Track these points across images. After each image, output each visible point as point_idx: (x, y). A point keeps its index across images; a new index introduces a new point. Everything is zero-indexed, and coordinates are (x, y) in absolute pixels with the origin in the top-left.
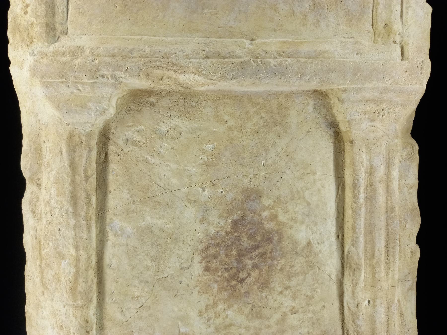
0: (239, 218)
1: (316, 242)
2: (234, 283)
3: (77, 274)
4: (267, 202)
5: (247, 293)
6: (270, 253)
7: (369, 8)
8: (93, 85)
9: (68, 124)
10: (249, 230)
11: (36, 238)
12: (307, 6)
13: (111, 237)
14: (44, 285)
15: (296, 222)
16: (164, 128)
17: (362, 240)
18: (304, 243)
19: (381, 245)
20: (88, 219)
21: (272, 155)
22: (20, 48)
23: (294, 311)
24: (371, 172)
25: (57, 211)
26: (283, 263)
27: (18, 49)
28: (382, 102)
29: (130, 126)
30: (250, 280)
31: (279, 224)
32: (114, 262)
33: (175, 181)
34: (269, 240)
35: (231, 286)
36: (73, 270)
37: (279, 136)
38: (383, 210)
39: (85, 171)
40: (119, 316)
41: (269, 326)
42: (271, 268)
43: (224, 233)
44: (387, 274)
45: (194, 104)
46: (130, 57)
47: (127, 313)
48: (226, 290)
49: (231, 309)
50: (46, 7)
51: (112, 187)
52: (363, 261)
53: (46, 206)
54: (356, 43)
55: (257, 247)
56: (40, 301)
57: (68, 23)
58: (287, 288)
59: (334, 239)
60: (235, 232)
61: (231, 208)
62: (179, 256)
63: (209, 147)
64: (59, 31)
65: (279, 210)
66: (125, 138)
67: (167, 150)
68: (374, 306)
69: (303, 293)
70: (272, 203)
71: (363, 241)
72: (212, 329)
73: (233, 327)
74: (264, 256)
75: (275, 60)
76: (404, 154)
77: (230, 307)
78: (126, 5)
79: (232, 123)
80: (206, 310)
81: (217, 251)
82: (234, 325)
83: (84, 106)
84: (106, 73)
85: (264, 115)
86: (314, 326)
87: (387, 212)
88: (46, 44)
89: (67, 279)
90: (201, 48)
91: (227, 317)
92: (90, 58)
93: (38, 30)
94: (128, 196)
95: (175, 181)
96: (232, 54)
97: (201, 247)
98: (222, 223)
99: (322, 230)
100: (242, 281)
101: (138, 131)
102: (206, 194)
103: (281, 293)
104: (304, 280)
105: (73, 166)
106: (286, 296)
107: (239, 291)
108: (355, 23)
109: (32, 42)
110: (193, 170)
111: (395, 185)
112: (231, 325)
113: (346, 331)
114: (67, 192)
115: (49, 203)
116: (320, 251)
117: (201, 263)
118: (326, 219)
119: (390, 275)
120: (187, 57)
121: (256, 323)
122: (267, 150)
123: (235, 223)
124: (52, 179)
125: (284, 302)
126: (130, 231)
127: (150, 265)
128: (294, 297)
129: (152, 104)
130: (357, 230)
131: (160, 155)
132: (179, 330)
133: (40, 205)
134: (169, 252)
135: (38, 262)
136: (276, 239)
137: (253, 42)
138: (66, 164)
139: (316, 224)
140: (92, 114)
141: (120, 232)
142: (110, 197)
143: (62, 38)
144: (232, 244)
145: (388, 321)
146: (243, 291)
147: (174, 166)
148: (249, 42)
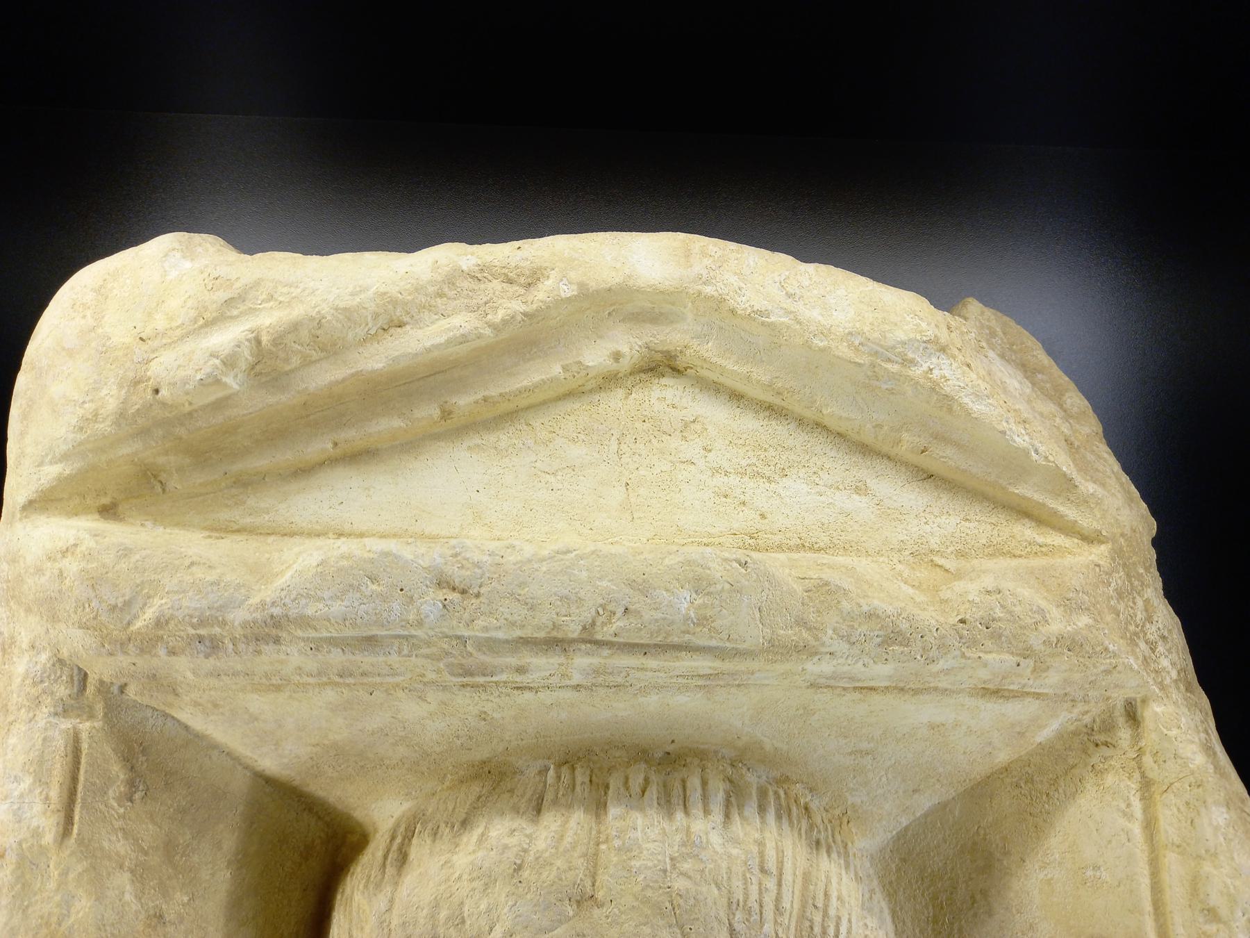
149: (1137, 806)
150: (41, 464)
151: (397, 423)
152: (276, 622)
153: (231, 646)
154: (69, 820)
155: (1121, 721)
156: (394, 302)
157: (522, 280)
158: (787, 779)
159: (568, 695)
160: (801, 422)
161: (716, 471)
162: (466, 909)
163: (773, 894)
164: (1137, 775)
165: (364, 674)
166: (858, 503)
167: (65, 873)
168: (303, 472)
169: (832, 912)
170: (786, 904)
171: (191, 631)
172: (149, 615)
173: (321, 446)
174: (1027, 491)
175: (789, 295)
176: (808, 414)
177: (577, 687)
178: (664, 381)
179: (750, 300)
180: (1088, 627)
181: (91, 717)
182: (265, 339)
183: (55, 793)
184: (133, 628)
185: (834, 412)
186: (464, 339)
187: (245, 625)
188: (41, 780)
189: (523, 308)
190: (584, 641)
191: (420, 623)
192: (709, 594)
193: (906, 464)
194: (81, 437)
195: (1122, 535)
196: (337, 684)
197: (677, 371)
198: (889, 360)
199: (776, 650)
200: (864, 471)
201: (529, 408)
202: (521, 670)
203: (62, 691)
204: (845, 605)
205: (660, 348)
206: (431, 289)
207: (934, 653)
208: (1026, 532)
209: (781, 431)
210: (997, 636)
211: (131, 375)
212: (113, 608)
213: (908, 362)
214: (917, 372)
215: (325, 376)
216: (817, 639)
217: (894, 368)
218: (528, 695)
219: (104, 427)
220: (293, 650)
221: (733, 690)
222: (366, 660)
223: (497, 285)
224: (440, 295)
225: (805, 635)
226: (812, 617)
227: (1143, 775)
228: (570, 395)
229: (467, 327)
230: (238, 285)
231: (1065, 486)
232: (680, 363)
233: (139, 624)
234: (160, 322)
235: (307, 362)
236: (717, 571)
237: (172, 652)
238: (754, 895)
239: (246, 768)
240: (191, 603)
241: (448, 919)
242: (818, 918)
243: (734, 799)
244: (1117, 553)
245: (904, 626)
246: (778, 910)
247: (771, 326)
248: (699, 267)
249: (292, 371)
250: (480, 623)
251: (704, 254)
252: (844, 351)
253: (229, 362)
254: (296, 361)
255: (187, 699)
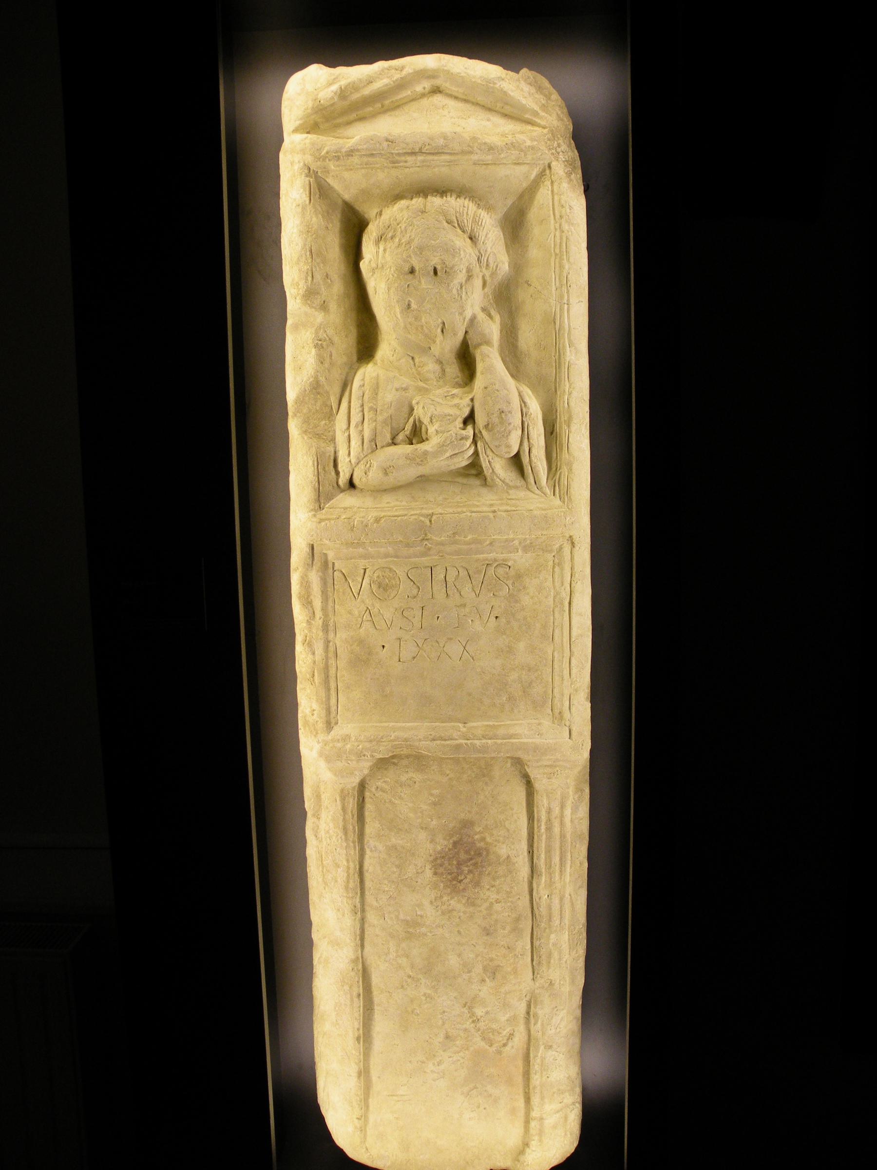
0: (458, 840)
1: (513, 855)
2: (454, 882)
3: (348, 875)
4: (477, 829)
5: (464, 890)
6: (480, 863)
7: (549, 698)
8: (358, 761)
9: (341, 784)
10: (465, 848)
11: (319, 853)
12: (504, 699)
13: (368, 851)
14: (326, 883)
15: (499, 843)
16: (403, 778)
17: (543, 856)
18: (505, 856)
19: (556, 859)
20: (354, 842)
21: (482, 797)
22: (309, 737)
23: (497, 901)
24: (549, 811)
25: (334, 838)
26: (490, 870)
27: (308, 737)
28: (555, 766)
29: (379, 779)
30: (467, 880)
31: (487, 843)
32: (371, 869)
33: (411, 815)
34: (480, 854)
35: (453, 885)
36: (346, 875)
37: (486, 784)
38: (558, 837)
39: (352, 812)
40: (375, 904)
41: (480, 911)
42: (481, 874)
43: (447, 850)
44: (561, 878)
45: (424, 763)
46: (381, 742)
47: (380, 902)
48: (449, 887)
49: (453, 900)
50: (326, 711)
51: (368, 819)
52: (543, 870)
53: (326, 834)
54: (539, 724)
55: (471, 859)
56: (322, 893)
57: (338, 716)
58: (492, 887)
59: (526, 854)
60: (456, 849)
61: (452, 833)
62: (416, 865)
63: (436, 792)
64: (333, 723)
65: (487, 834)
66: (376, 787)
67: (405, 794)
68: (551, 899)
69: (505, 889)
70: (482, 830)
71: (544, 858)
72: (440, 912)
73: (454, 911)
74: (476, 865)
75: (480, 741)
76: (576, 797)
77: (452, 898)
78: (377, 703)
79: (452, 775)
80: (435, 900)
81: (442, 861)
82: (455, 910)
83: (352, 774)
84: (367, 753)
85: (475, 770)
86: (512, 911)
87: (561, 837)
88: (326, 734)
89: (342, 880)
90: (429, 733)
91: (450, 905)
92: (356, 744)
93: (321, 725)
94: (379, 826)
95: (411, 815)
96: (451, 737)
97: (431, 859)
98: (446, 843)
99: (518, 848)
100: (460, 881)
101: (385, 782)
102: (434, 822)
103: (489, 889)
104: (505, 881)
105: (344, 809)
106: (492, 891)
107: (459, 887)
108: (539, 709)
109: (317, 733)
110: (424, 807)
111: (567, 820)
112: (453, 910)
113: (534, 915)
114: (341, 826)
115: (328, 832)
116: (517, 862)
117: (431, 869)
118: (521, 841)
119: (563, 879)
120: (420, 740)
121: (471, 909)
122: (478, 793)
123: (455, 844)
124: (330, 817)
125: (491, 896)
126: (381, 848)
127: (395, 870)
128: (498, 892)
129: (394, 764)
130: (540, 850)
131: (401, 798)
132: (417, 914)
133: (320, 832)
134: (408, 862)
135: (321, 869)
136: (485, 853)
137: (466, 725)
138: (339, 808)
139: (513, 844)
140: (357, 778)
141: (373, 849)
142: (367, 826)
143: (335, 727)
144: (453, 857)
145: (561, 908)
146: (461, 888)
147: (411, 805)
148: (463, 725)
149: (550, 187)
150: (296, 121)
151: (371, 109)
152: (352, 151)
153: (342, 158)
154: (310, 200)
155: (547, 168)
156: (370, 77)
157: (400, 69)
158: (474, 197)
159: (417, 169)
160: (473, 103)
161: (452, 118)
162: (397, 217)
163: (466, 211)
164: (550, 181)
165: (371, 164)
166: (488, 123)
167: (311, 211)
168: (349, 123)
169: (481, 217)
170: (469, 212)
171: (334, 154)
172: (325, 151)
173: (353, 116)
174: (527, 116)
175: (466, 68)
176: (474, 100)
177: (419, 167)
178: (437, 95)
179: (455, 70)
180: (537, 144)
181: (312, 178)
182: (343, 87)
183: (308, 193)
184: (321, 155)
185: (480, 99)
186: (387, 85)
187: (345, 152)
188: (305, 190)
189: (401, 76)
190: (420, 152)
191: (383, 150)
192: (447, 140)
193: (500, 113)
194: (305, 114)
195: (554, 127)
196: (364, 168)
197: (440, 92)
198: (490, 83)
199: (463, 152)
200: (489, 115)
201: (403, 104)
202: (406, 162)
203: (306, 171)
204: (479, 141)
205: (435, 85)
206: (378, 73)
207: (500, 152)
208: (529, 127)
209: (468, 106)
210: (514, 147)
211: (314, 98)
212: (318, 150)
213: (495, 84)
214: (497, 86)
215: (356, 96)
216: (473, 149)
217: (492, 85)
218: (408, 169)
219: (309, 111)
220: (356, 158)
221: (456, 166)
222: (371, 159)
223: (393, 71)
224: (380, 74)
225: (470, 148)
226: (471, 144)
227: (552, 180)
228: (414, 100)
229: (387, 82)
230: (336, 75)
231: (536, 114)
232: (441, 89)
233: (323, 154)
234: (319, 85)
235: (351, 93)
236: (449, 134)
237: (329, 160)
238: (461, 210)
239: (342, 198)
240: (333, 148)
241: (393, 220)
242: (477, 218)
243: (459, 196)
244: (552, 132)
245: (492, 145)
246: (467, 214)
247: (462, 76)
248: (443, 62)
249: (348, 95)
250: (396, 148)
251: (444, 59)
252: (479, 81)
253: (335, 93)
254: (349, 92)
255: (331, 174)
